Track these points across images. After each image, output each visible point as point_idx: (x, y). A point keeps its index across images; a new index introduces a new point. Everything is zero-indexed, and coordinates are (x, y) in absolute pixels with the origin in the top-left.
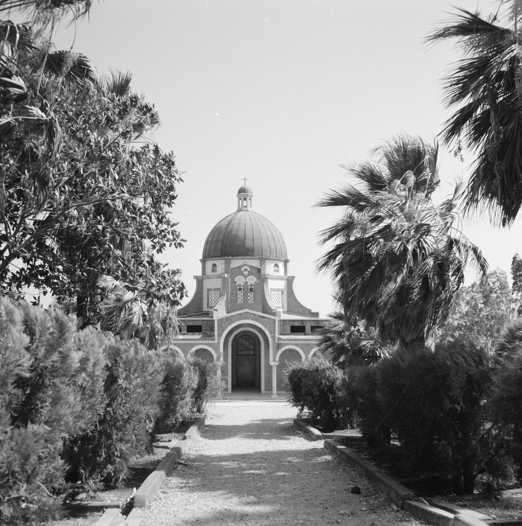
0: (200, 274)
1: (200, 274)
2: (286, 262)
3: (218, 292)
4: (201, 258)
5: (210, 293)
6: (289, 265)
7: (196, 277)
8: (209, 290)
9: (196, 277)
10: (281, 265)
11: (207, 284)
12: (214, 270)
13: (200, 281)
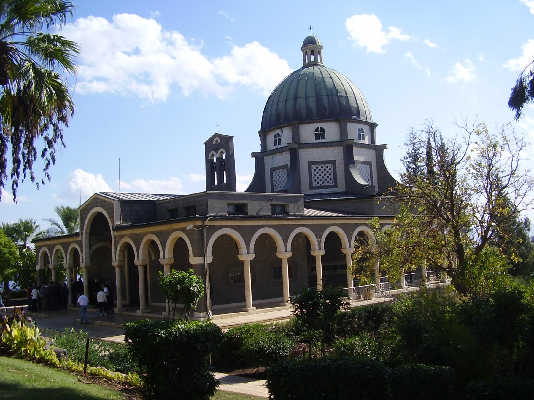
0: (258, 149)
1: (258, 149)
2: (373, 126)
3: (285, 171)
4: (259, 128)
5: (274, 173)
6: (377, 130)
7: (254, 155)
8: (273, 170)
9: (254, 155)
10: (366, 129)
11: (270, 162)
12: (278, 141)
13: (259, 158)
